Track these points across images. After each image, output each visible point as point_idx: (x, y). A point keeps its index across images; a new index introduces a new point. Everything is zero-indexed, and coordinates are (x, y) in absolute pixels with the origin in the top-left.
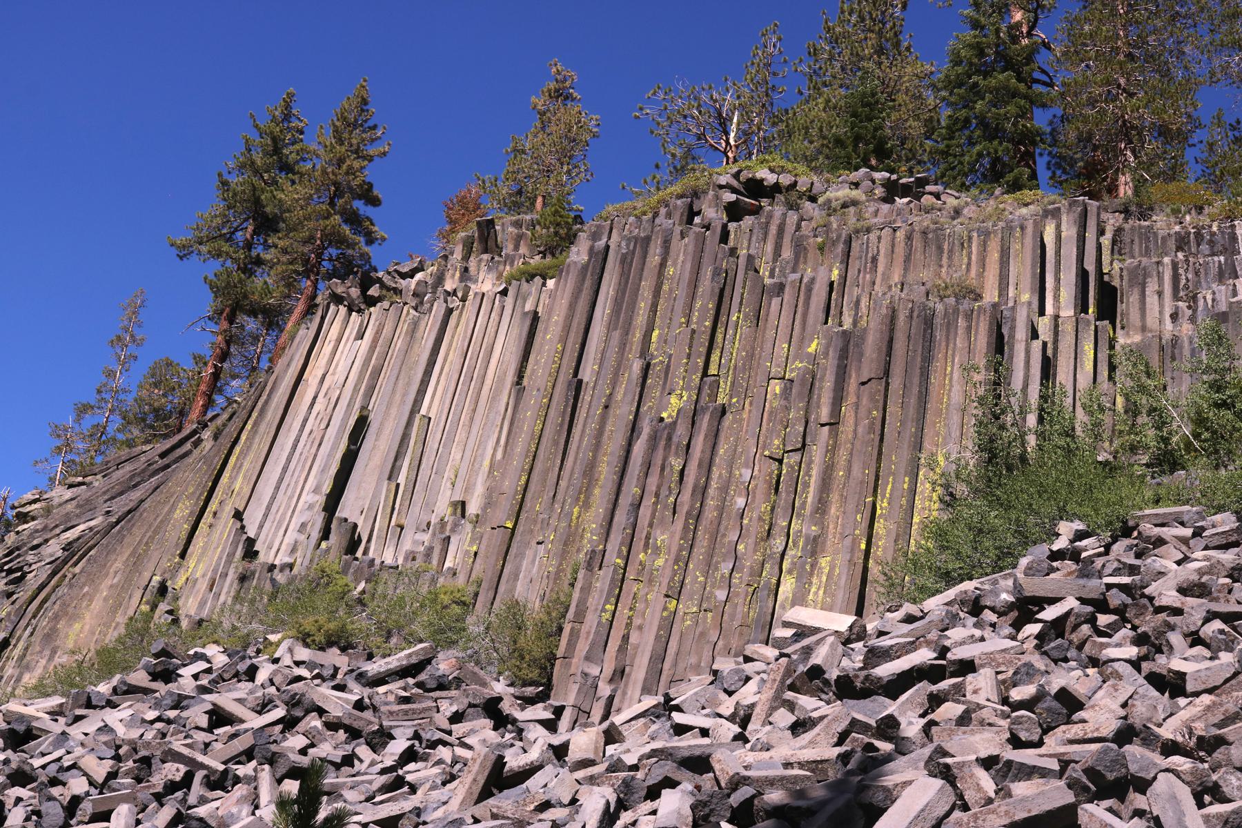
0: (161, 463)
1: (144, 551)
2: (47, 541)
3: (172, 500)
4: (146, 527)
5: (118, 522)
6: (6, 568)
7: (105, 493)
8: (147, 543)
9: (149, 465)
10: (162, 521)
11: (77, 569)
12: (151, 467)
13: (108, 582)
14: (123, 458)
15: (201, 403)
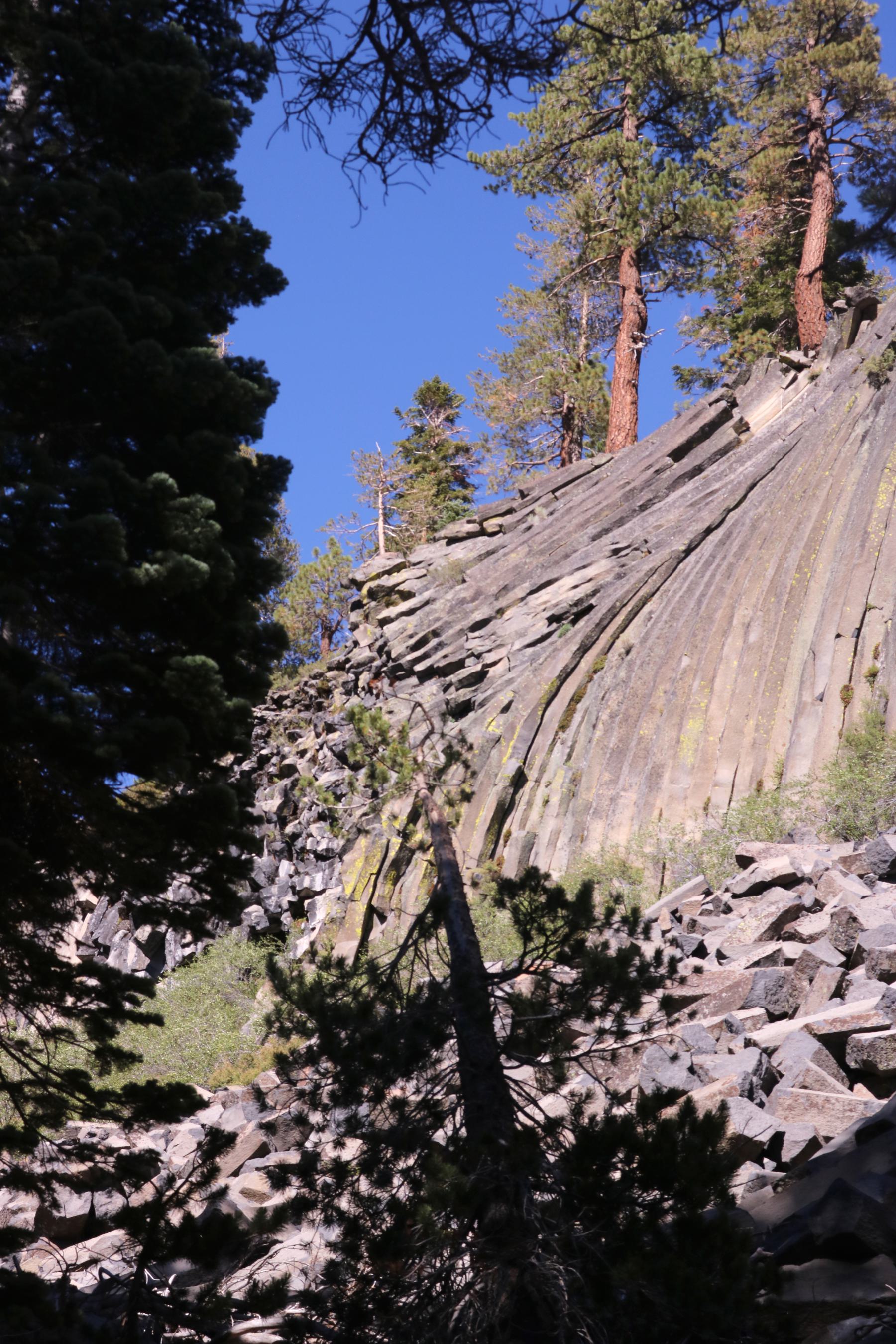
0: (680, 468)
1: (799, 581)
2: (501, 612)
3: (822, 494)
4: (778, 548)
5: (688, 551)
6: (419, 667)
7: (583, 525)
8: (799, 569)
9: (657, 472)
10: (815, 529)
11: (631, 635)
12: (664, 475)
13: (734, 642)
14: (561, 481)
15: (629, 399)
